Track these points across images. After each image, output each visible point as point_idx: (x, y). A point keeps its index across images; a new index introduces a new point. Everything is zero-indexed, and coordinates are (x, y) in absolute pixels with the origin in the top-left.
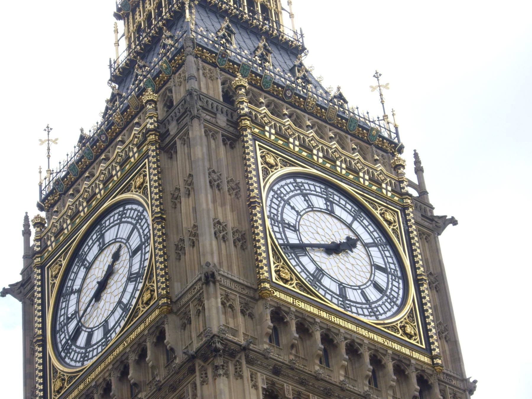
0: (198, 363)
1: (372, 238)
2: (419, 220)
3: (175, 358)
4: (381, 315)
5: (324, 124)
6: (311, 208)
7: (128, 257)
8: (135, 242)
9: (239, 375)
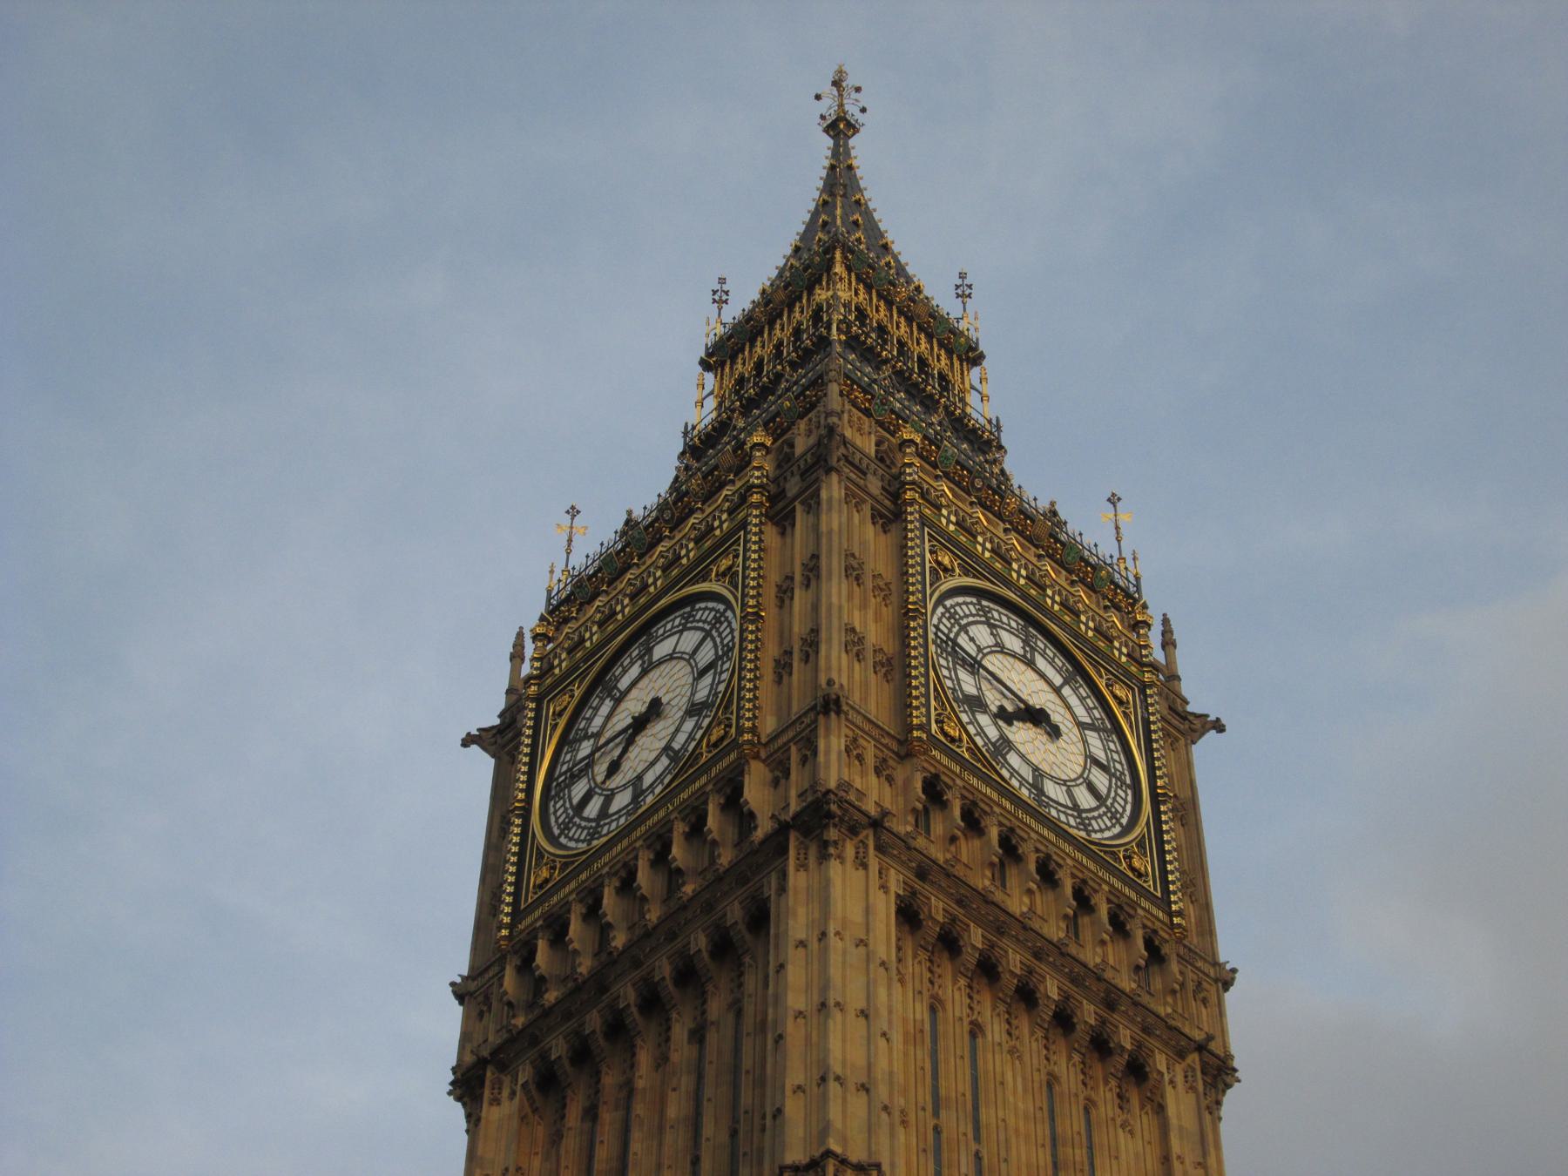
2: (1165, 712)
3: (756, 827)
6: (1000, 648)
7: (690, 680)
8: (706, 655)
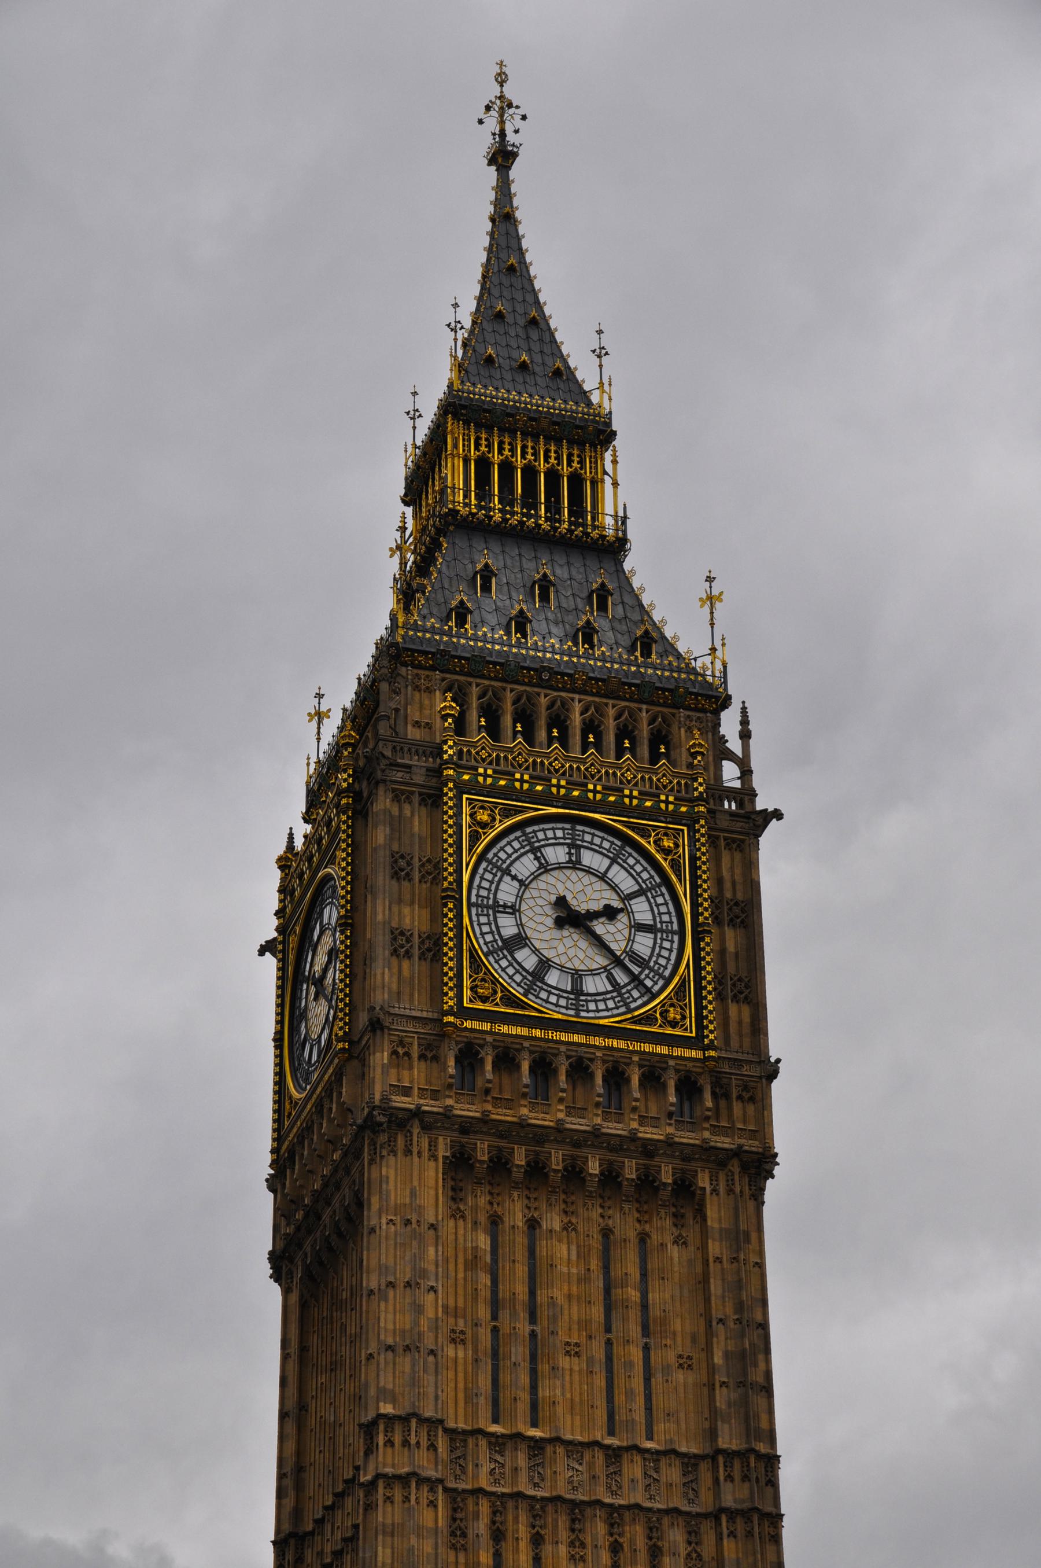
0: (368, 1133)
1: (638, 882)
4: (635, 1000)
5: (605, 700)
6: (545, 868)
9: (408, 1152)
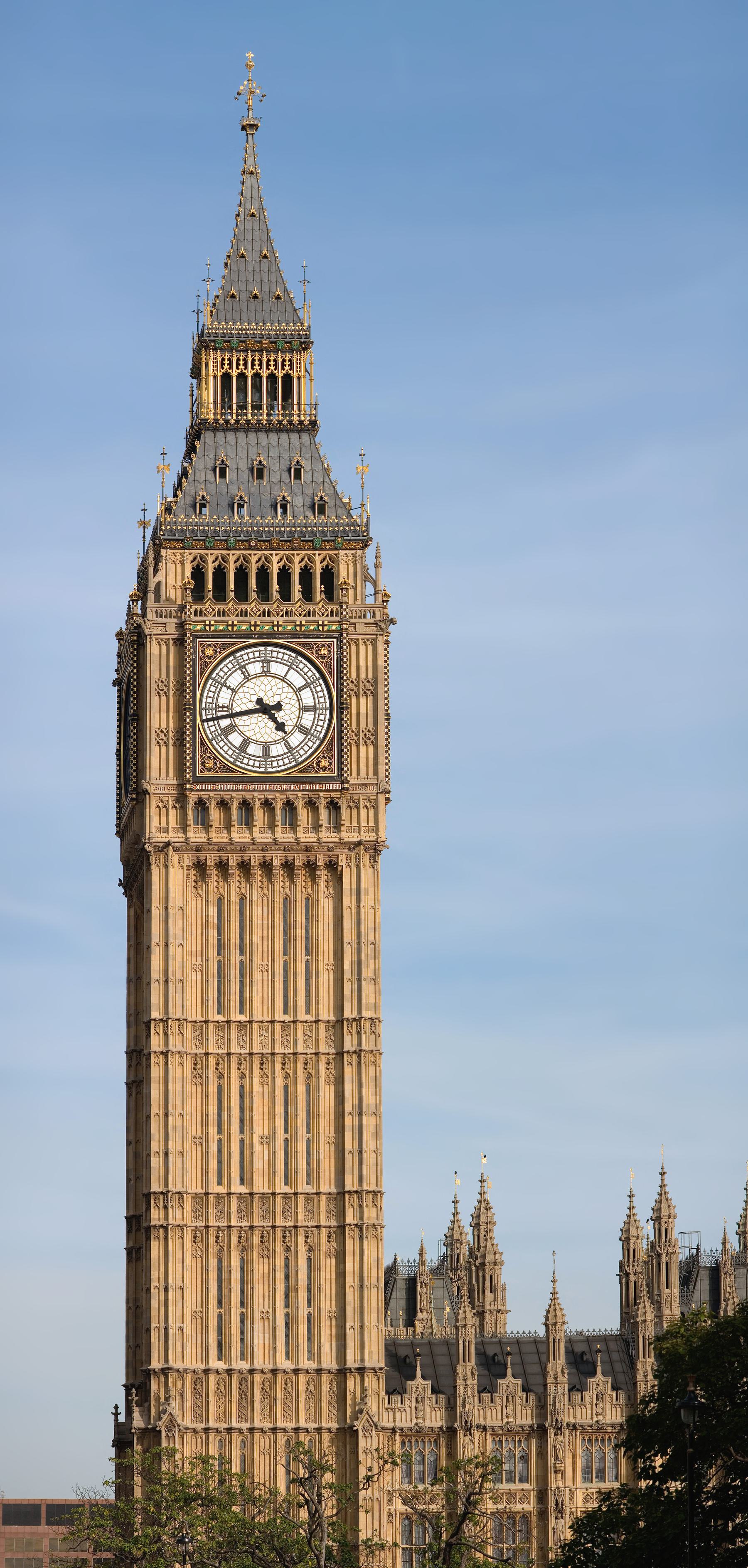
5: (292, 552)
6: (247, 678)
